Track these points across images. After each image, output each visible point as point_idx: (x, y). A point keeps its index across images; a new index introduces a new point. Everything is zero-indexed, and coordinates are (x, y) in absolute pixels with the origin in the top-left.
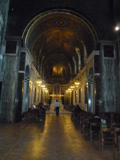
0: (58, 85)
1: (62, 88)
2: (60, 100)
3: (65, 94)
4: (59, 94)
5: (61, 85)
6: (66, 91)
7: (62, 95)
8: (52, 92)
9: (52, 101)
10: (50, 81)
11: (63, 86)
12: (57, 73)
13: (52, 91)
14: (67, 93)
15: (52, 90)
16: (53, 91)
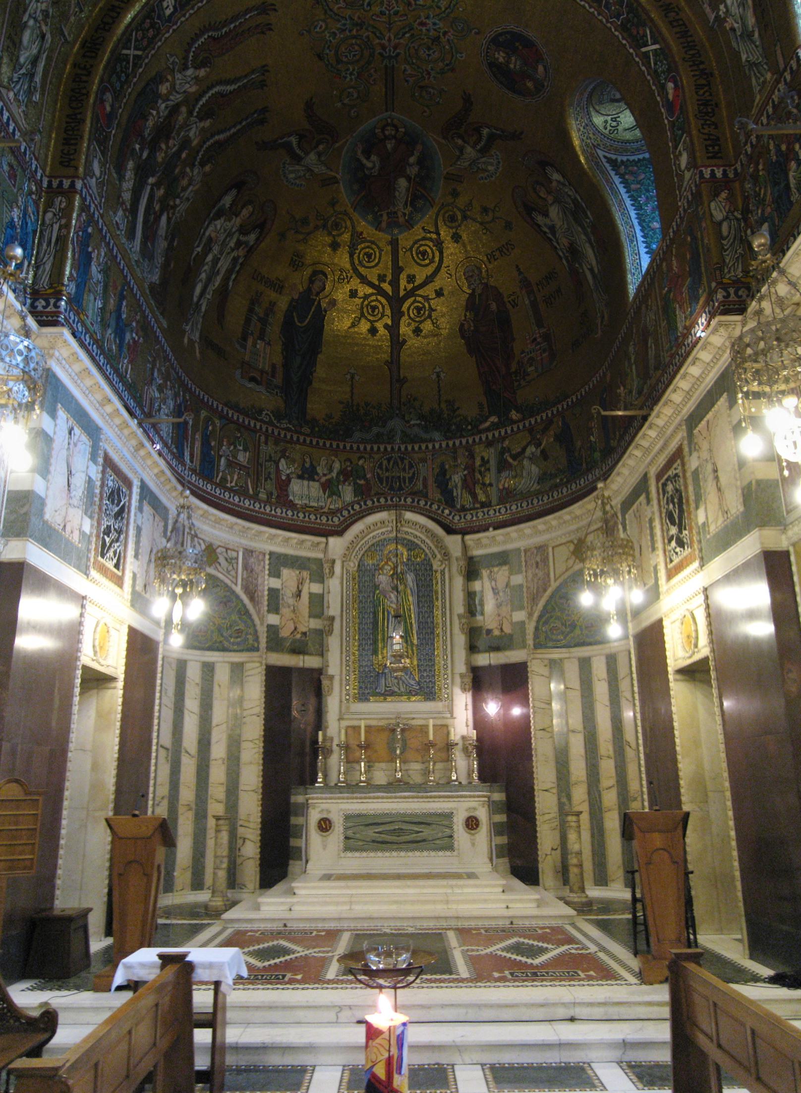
0: (411, 546)
1: (483, 586)
2: (447, 785)
3: (535, 685)
4: (428, 691)
5: (453, 542)
6: (586, 599)
7: (492, 708)
8: (311, 662)
9: (314, 816)
10: (283, 486)
11: (502, 559)
12: (394, 362)
13: (322, 655)
14: (614, 631)
15: (315, 624)
16: (334, 643)
